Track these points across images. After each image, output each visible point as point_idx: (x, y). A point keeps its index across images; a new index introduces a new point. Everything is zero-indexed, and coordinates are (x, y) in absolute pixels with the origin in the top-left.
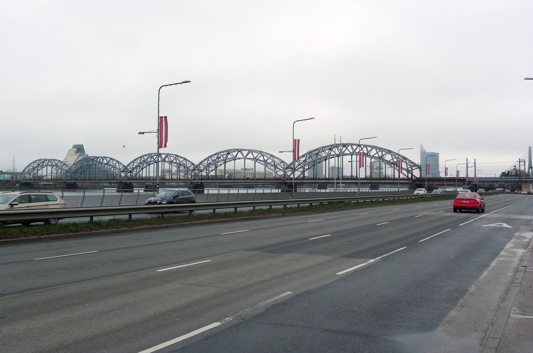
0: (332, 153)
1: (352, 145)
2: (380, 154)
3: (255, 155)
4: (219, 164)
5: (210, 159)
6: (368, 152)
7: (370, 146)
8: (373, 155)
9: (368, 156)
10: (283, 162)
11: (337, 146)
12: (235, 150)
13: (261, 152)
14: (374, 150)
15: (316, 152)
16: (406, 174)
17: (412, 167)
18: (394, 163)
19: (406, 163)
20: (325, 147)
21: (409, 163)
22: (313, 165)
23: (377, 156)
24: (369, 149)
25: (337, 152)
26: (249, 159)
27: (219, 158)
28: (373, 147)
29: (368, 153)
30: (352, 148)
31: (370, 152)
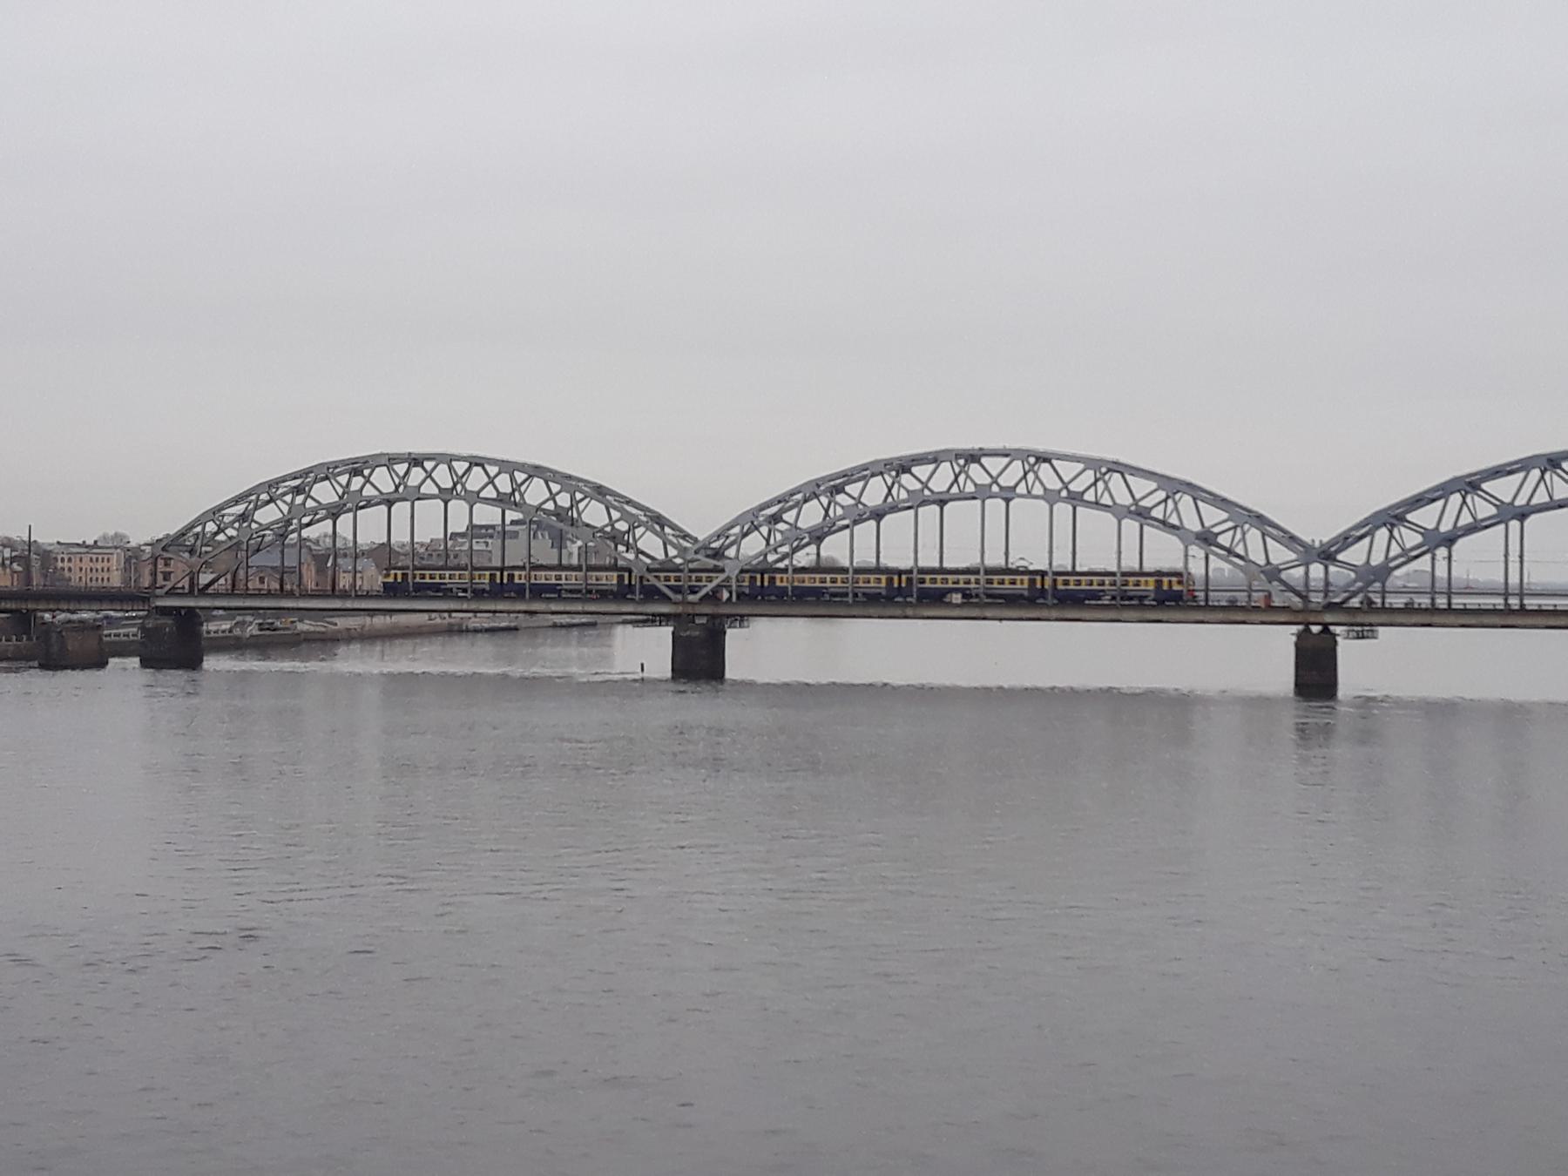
0: (369, 491)
1: (449, 459)
6: (516, 487)
7: (522, 467)
8: (536, 503)
9: (516, 504)
11: (391, 461)
14: (538, 483)
15: (297, 482)
18: (614, 538)
19: (662, 535)
20: (336, 465)
21: (675, 540)
22: (282, 535)
23: (550, 506)
24: (520, 477)
28: (535, 471)
29: (514, 491)
30: (451, 468)
31: (523, 488)
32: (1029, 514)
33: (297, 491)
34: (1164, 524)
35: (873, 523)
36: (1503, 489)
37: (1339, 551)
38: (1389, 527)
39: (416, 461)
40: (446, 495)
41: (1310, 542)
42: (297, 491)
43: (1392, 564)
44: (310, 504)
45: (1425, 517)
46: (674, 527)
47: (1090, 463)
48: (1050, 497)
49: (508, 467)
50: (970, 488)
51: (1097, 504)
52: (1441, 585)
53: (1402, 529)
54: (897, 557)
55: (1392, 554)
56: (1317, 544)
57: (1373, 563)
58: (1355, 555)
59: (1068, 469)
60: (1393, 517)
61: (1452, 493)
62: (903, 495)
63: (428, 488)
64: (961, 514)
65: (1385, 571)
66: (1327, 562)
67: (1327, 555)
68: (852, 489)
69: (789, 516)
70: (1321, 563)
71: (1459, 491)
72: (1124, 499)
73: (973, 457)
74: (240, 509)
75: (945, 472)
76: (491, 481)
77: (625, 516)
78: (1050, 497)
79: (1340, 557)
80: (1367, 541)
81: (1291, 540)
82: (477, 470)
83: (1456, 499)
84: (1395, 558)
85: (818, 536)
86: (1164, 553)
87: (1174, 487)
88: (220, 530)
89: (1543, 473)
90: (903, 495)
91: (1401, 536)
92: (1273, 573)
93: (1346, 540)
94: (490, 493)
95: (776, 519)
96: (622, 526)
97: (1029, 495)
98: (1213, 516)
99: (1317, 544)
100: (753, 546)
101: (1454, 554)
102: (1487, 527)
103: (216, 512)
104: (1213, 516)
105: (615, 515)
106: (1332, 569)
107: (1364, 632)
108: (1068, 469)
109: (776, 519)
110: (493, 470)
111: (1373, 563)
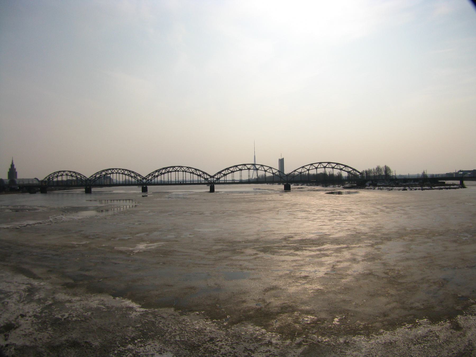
0: (108, 173)
2: (129, 173)
3: (72, 173)
4: (54, 178)
5: (50, 176)
10: (85, 177)
11: (110, 169)
12: (62, 171)
13: (74, 172)
16: (140, 182)
17: (142, 179)
23: (128, 174)
24: (124, 171)
25: (110, 172)
26: (69, 175)
27: (54, 175)
28: (126, 170)
30: (117, 170)
32: (181, 173)
33: (101, 173)
34: (195, 174)
35: (163, 175)
39: (113, 169)
40: (116, 173)
42: (101, 173)
44: (102, 175)
45: (224, 172)
46: (141, 176)
47: (187, 167)
48: (183, 171)
49: (123, 170)
50: (174, 170)
51: (188, 172)
52: (225, 180)
54: (166, 179)
57: (218, 178)
58: (216, 177)
59: (185, 168)
60: (220, 173)
62: (167, 171)
63: (114, 172)
64: (173, 174)
65: (219, 178)
67: (213, 177)
68: (161, 171)
69: (154, 174)
72: (191, 171)
73: (174, 167)
74: (95, 175)
75: (171, 168)
76: (121, 171)
77: (136, 175)
78: (183, 171)
79: (215, 177)
80: (217, 175)
81: (209, 175)
82: (120, 170)
83: (227, 170)
85: (157, 176)
86: (196, 178)
87: (196, 170)
88: (93, 178)
90: (167, 171)
92: (207, 179)
93: (215, 175)
94: (121, 173)
95: (153, 174)
96: (136, 176)
97: (181, 171)
98: (201, 173)
100: (150, 178)
103: (92, 176)
104: (201, 173)
105: (135, 175)
108: (185, 168)
109: (153, 174)
110: (121, 170)
111: (218, 178)
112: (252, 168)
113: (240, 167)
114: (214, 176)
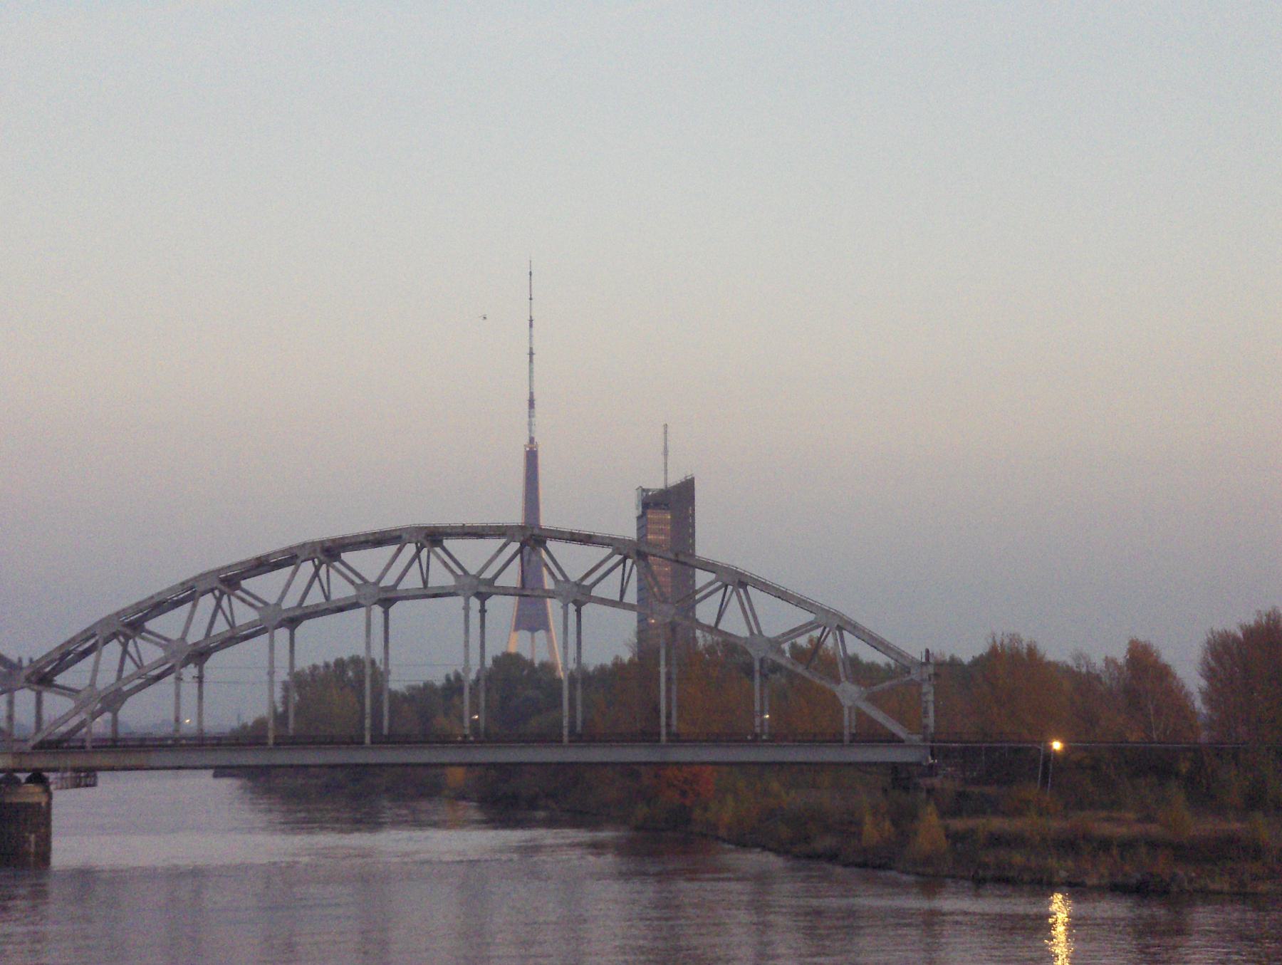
36: (266, 586)
37: (56, 671)
38: (122, 639)
41: (15, 660)
43: (125, 688)
53: (139, 641)
55: (125, 674)
56: (25, 663)
61: (203, 594)
66: (36, 687)
67: (42, 678)
70: (33, 690)
71: (212, 590)
79: (59, 680)
83: (207, 602)
84: (130, 679)
89: (317, 569)
91: (136, 646)
93: (66, 657)
99: (25, 663)
101: (207, 673)
102: (247, 637)
106: (48, 697)
107: (84, 777)
111: (100, 685)
112: (608, 588)
113: (368, 562)
114: (47, 658)
